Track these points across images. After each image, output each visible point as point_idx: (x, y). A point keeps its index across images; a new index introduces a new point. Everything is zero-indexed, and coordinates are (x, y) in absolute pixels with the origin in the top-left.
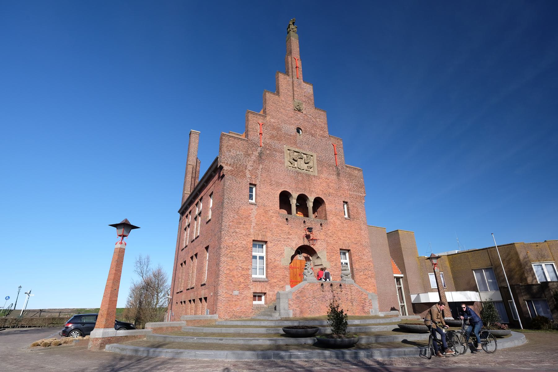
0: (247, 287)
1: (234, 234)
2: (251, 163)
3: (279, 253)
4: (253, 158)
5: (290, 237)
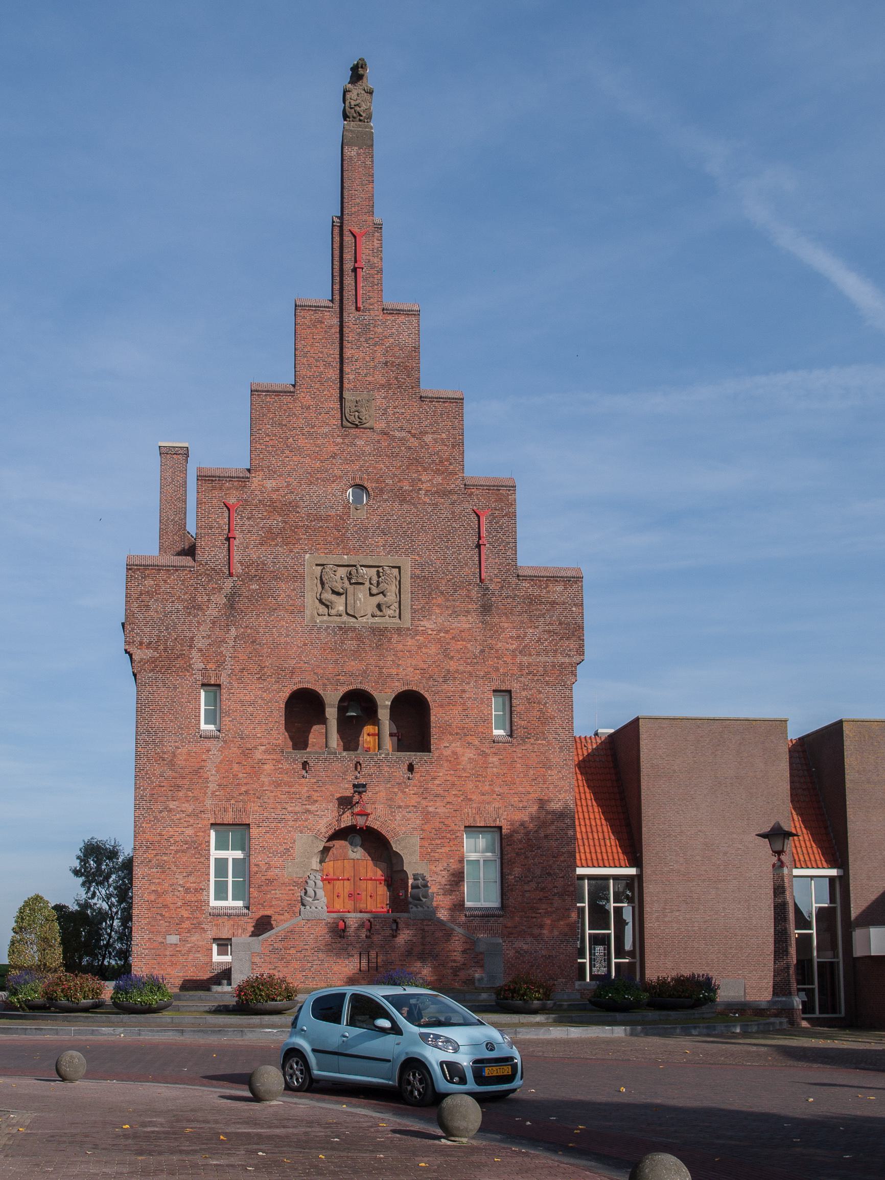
0: (198, 927)
1: (165, 814)
2: (204, 629)
3: (281, 849)
4: (212, 612)
5: (312, 808)
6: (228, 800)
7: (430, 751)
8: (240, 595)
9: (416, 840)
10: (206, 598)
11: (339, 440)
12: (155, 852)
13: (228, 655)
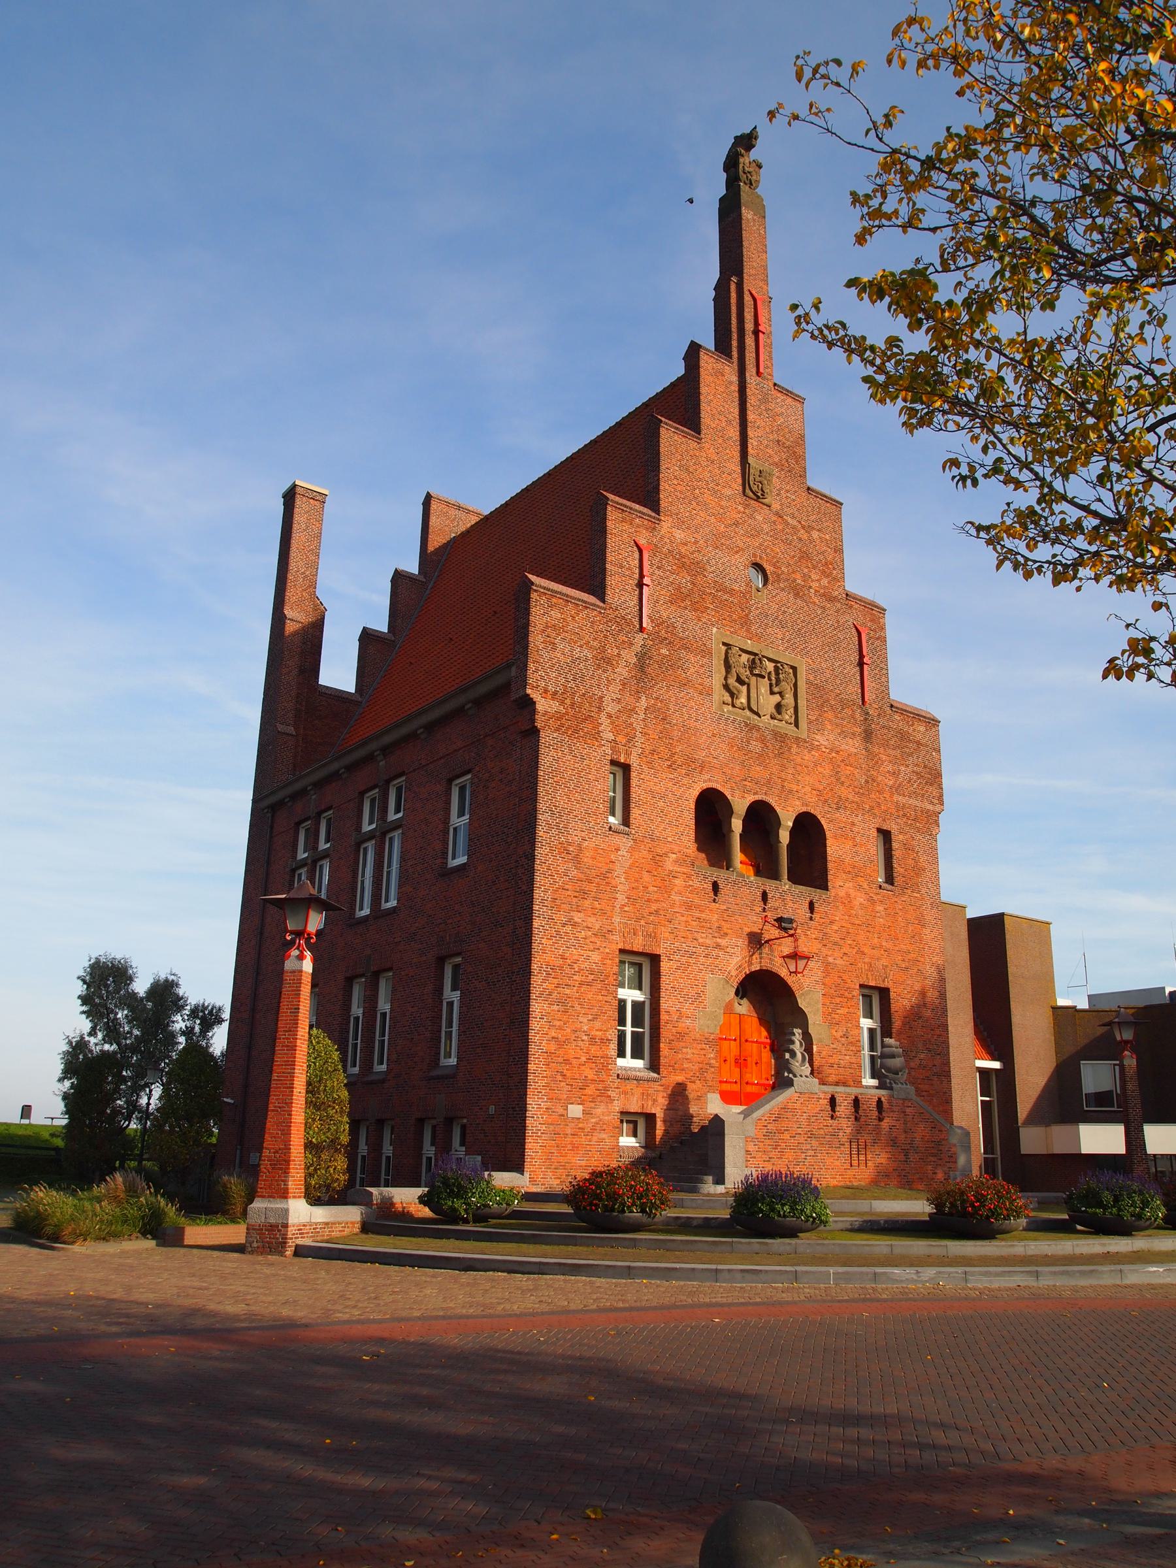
0: (603, 1095)
1: (568, 929)
2: (613, 692)
6: (638, 920)
7: (826, 888)
8: (650, 658)
9: (818, 996)
10: (616, 652)
11: (740, 508)
12: (556, 981)
13: (639, 729)
